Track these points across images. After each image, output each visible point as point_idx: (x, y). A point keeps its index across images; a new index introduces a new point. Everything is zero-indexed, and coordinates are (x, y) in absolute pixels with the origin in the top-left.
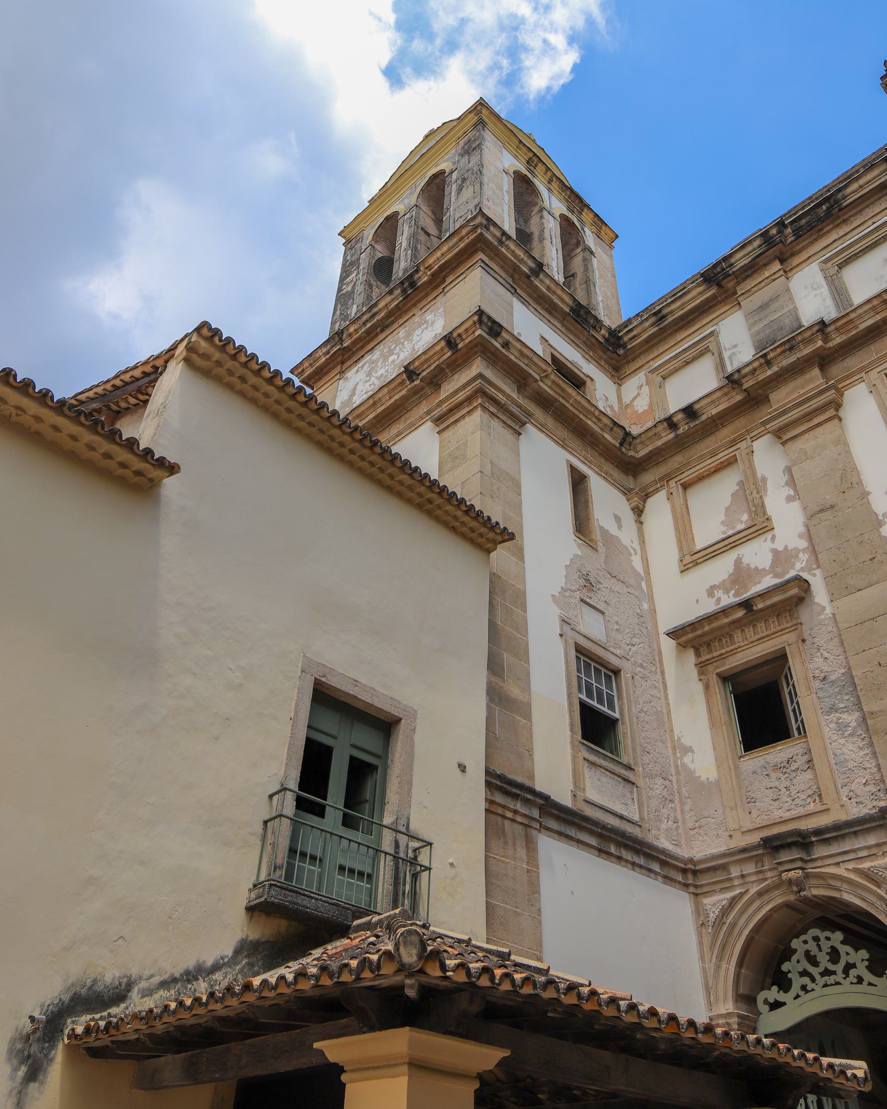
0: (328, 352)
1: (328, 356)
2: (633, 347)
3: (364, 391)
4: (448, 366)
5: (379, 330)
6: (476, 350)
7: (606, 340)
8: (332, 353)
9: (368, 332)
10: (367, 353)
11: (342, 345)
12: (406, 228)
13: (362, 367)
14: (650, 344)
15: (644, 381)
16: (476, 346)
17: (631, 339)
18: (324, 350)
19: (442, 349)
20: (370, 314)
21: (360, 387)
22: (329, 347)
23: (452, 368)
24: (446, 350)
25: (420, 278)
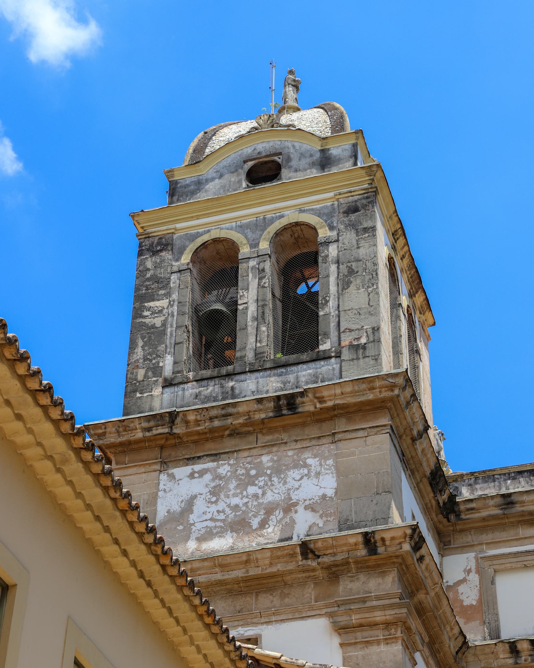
0: (149, 429)
1: (147, 434)
2: (467, 519)
3: (209, 516)
4: (356, 562)
5: (227, 432)
6: (395, 560)
7: (444, 503)
8: (155, 432)
9: (212, 430)
10: (207, 455)
11: (171, 428)
12: (254, 284)
13: (202, 473)
14: (486, 523)
15: (472, 565)
16: (397, 557)
17: (468, 510)
18: (145, 425)
19: (356, 544)
20: (223, 412)
21: (200, 506)
22: (152, 423)
23: (360, 565)
24: (361, 546)
25: (303, 403)
